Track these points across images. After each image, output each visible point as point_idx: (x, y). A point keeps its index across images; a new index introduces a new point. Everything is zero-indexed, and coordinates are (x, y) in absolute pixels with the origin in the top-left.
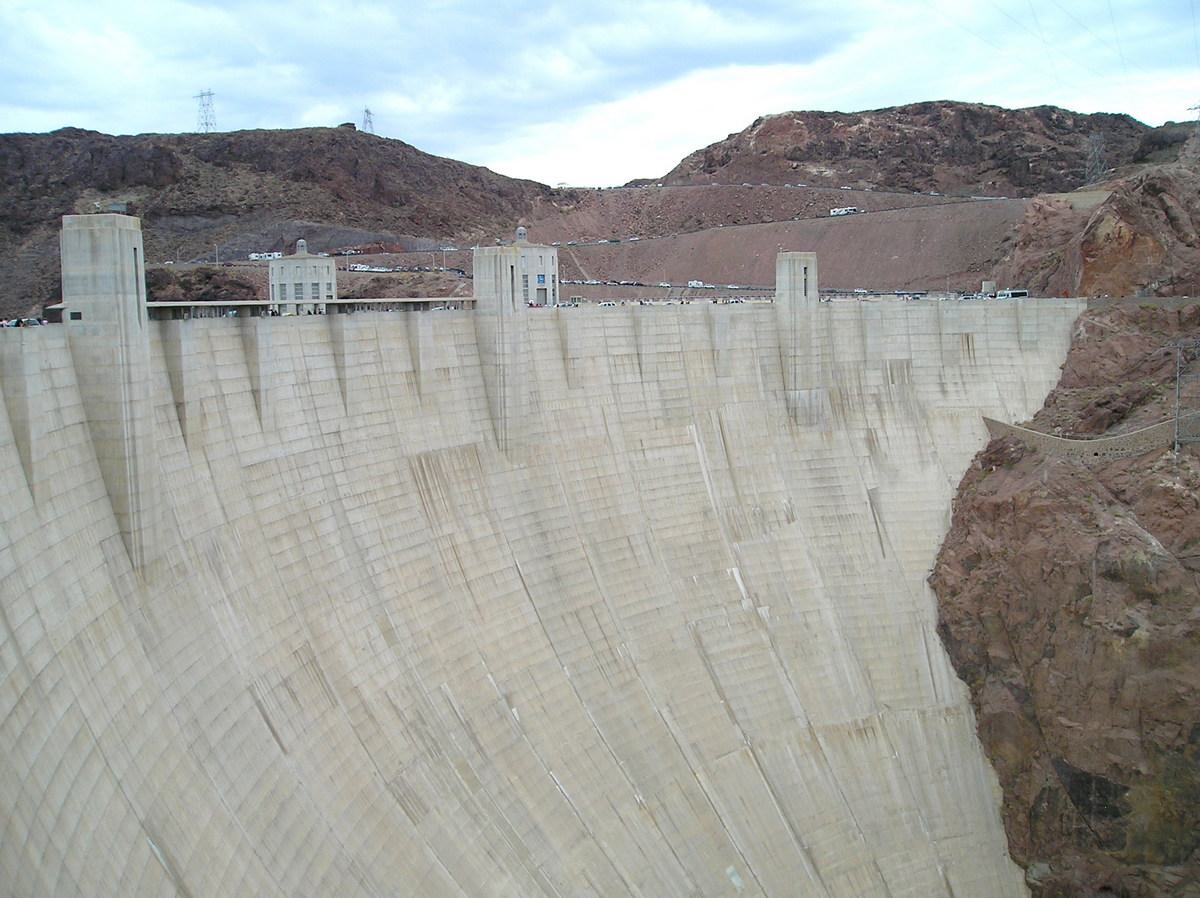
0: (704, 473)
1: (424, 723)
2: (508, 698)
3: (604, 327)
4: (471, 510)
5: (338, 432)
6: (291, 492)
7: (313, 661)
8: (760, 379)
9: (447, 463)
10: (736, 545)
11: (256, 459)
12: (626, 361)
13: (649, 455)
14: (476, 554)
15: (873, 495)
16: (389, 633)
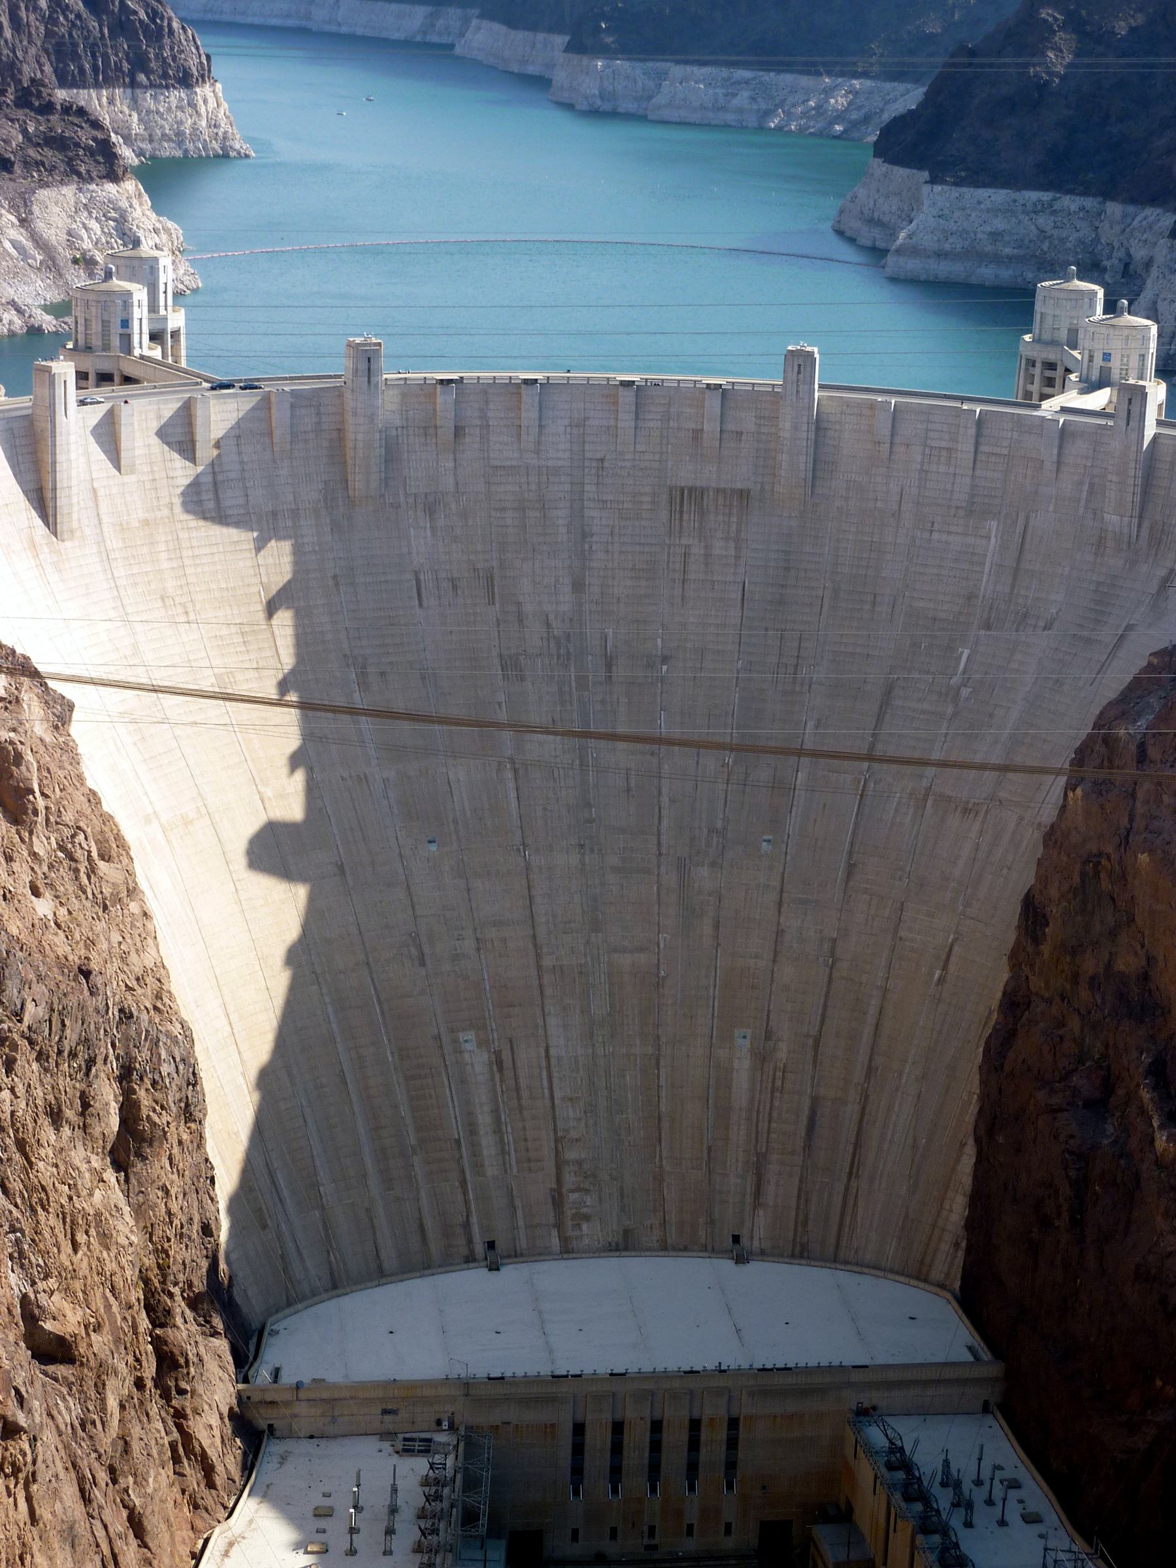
0: (988, 565)
1: (569, 641)
2: (665, 659)
3: (928, 421)
4: (719, 534)
5: (602, 460)
6: (533, 487)
7: (490, 579)
8: (1084, 495)
9: (711, 497)
10: (983, 632)
11: (508, 463)
12: (944, 453)
13: (935, 536)
14: (706, 564)
15: (1129, 628)
16: (578, 586)
